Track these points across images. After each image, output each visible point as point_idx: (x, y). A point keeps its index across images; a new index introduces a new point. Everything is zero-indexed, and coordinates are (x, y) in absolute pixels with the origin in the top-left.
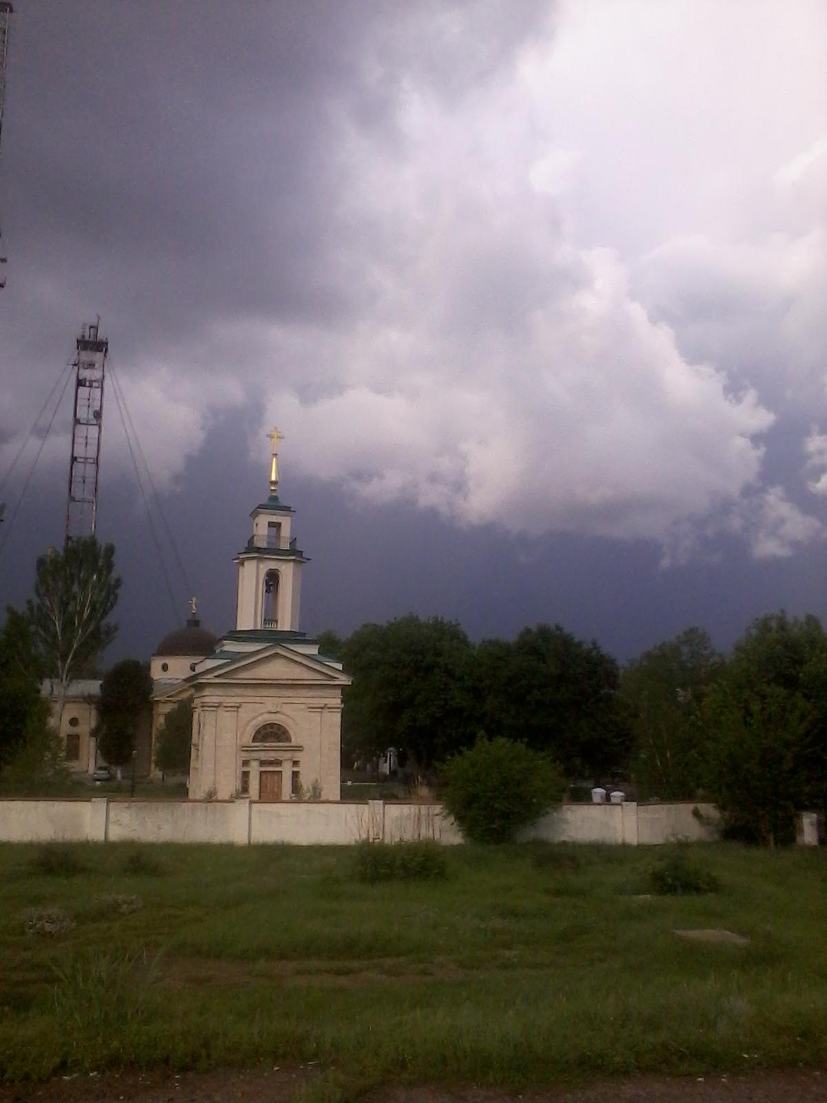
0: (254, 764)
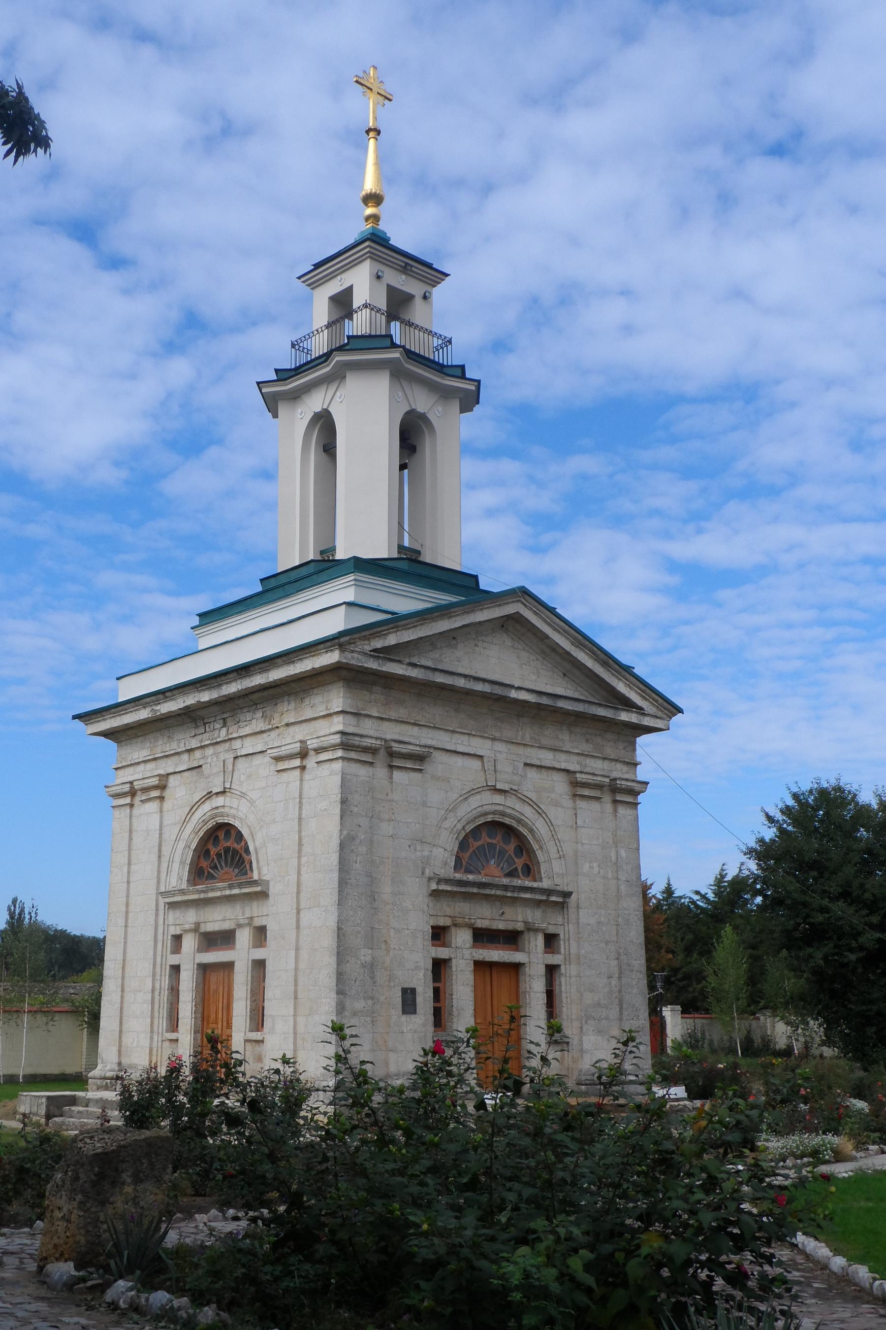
0: (462, 938)
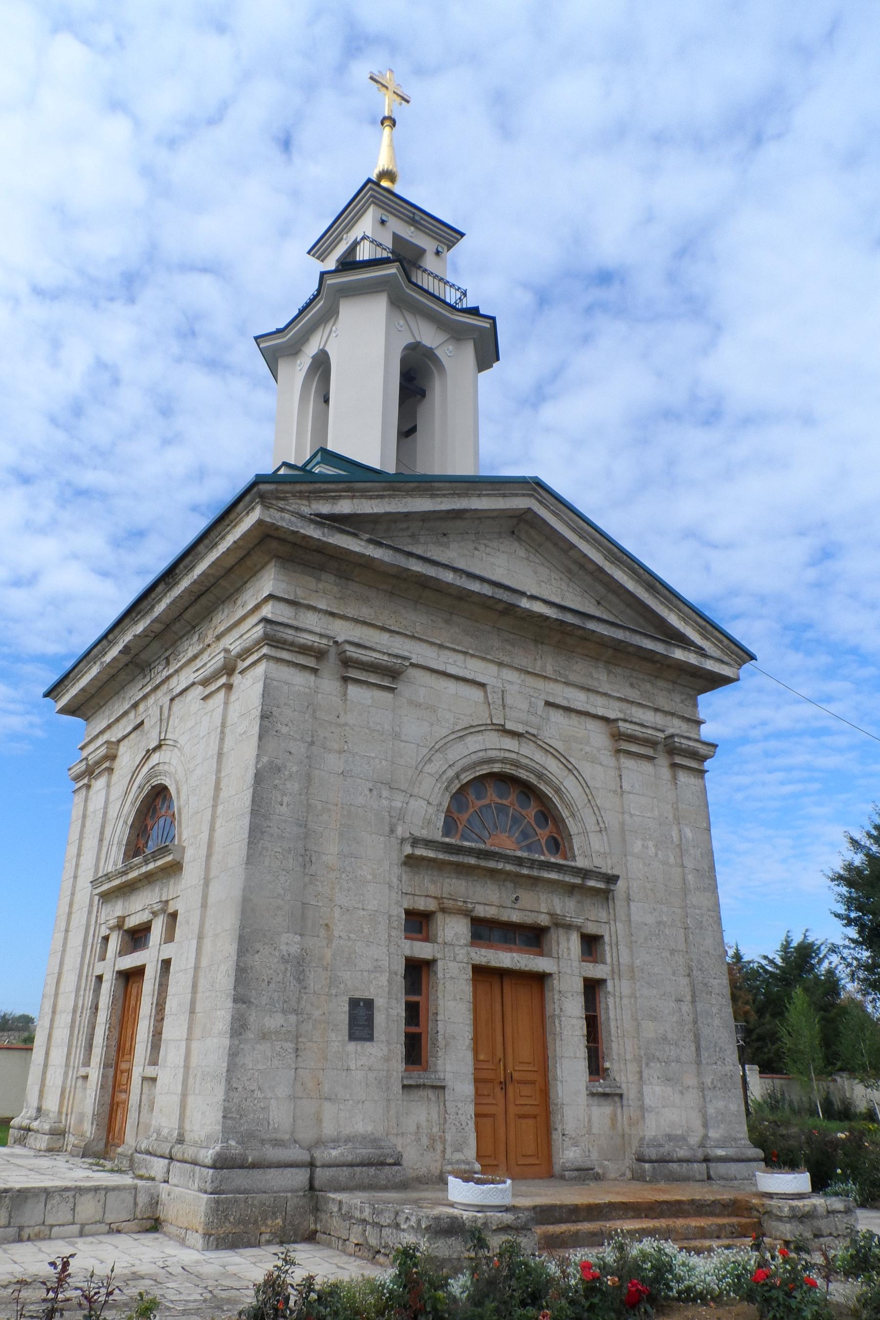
0: (453, 930)
